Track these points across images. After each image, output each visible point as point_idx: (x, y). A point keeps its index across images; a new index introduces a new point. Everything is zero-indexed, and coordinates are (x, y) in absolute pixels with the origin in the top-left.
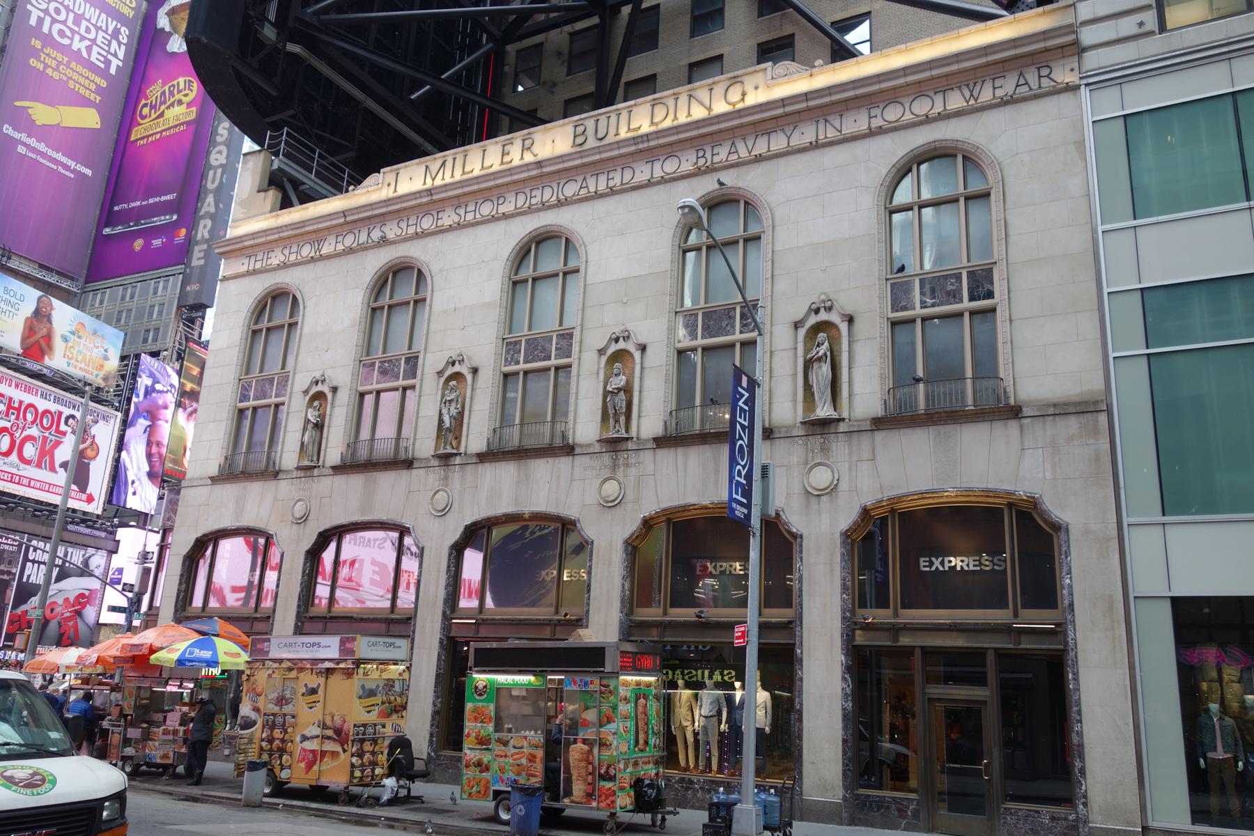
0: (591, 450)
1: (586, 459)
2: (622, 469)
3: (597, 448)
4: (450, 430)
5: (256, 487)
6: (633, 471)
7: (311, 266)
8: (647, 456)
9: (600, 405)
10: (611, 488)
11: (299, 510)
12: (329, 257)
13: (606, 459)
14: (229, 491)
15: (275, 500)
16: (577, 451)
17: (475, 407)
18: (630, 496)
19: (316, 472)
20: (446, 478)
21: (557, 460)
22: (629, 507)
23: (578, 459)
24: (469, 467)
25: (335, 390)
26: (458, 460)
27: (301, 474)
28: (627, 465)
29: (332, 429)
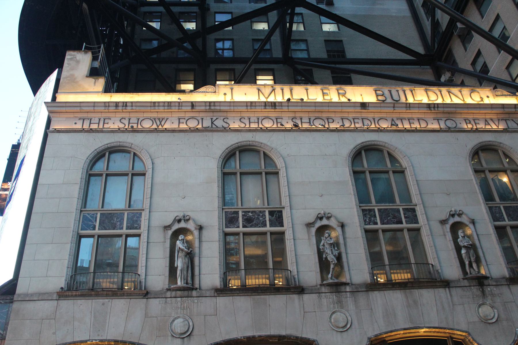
0: (462, 284)
1: (459, 290)
2: (490, 297)
3: (466, 283)
4: (330, 265)
5: (119, 304)
6: (498, 300)
7: (154, 135)
8: (505, 290)
9: (456, 256)
10: (486, 310)
11: (179, 325)
12: (166, 131)
13: (476, 290)
14: (83, 308)
15: (146, 315)
16: (452, 285)
17: (349, 251)
18: (503, 316)
19: (194, 293)
20: (340, 302)
21: (436, 290)
22: (505, 323)
23: (454, 291)
24: (360, 294)
25: (201, 228)
26: (348, 289)
27: (174, 293)
28: (493, 295)
29: (203, 260)
